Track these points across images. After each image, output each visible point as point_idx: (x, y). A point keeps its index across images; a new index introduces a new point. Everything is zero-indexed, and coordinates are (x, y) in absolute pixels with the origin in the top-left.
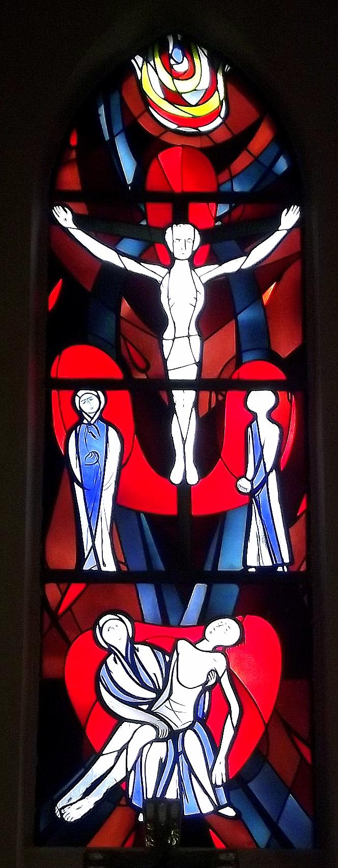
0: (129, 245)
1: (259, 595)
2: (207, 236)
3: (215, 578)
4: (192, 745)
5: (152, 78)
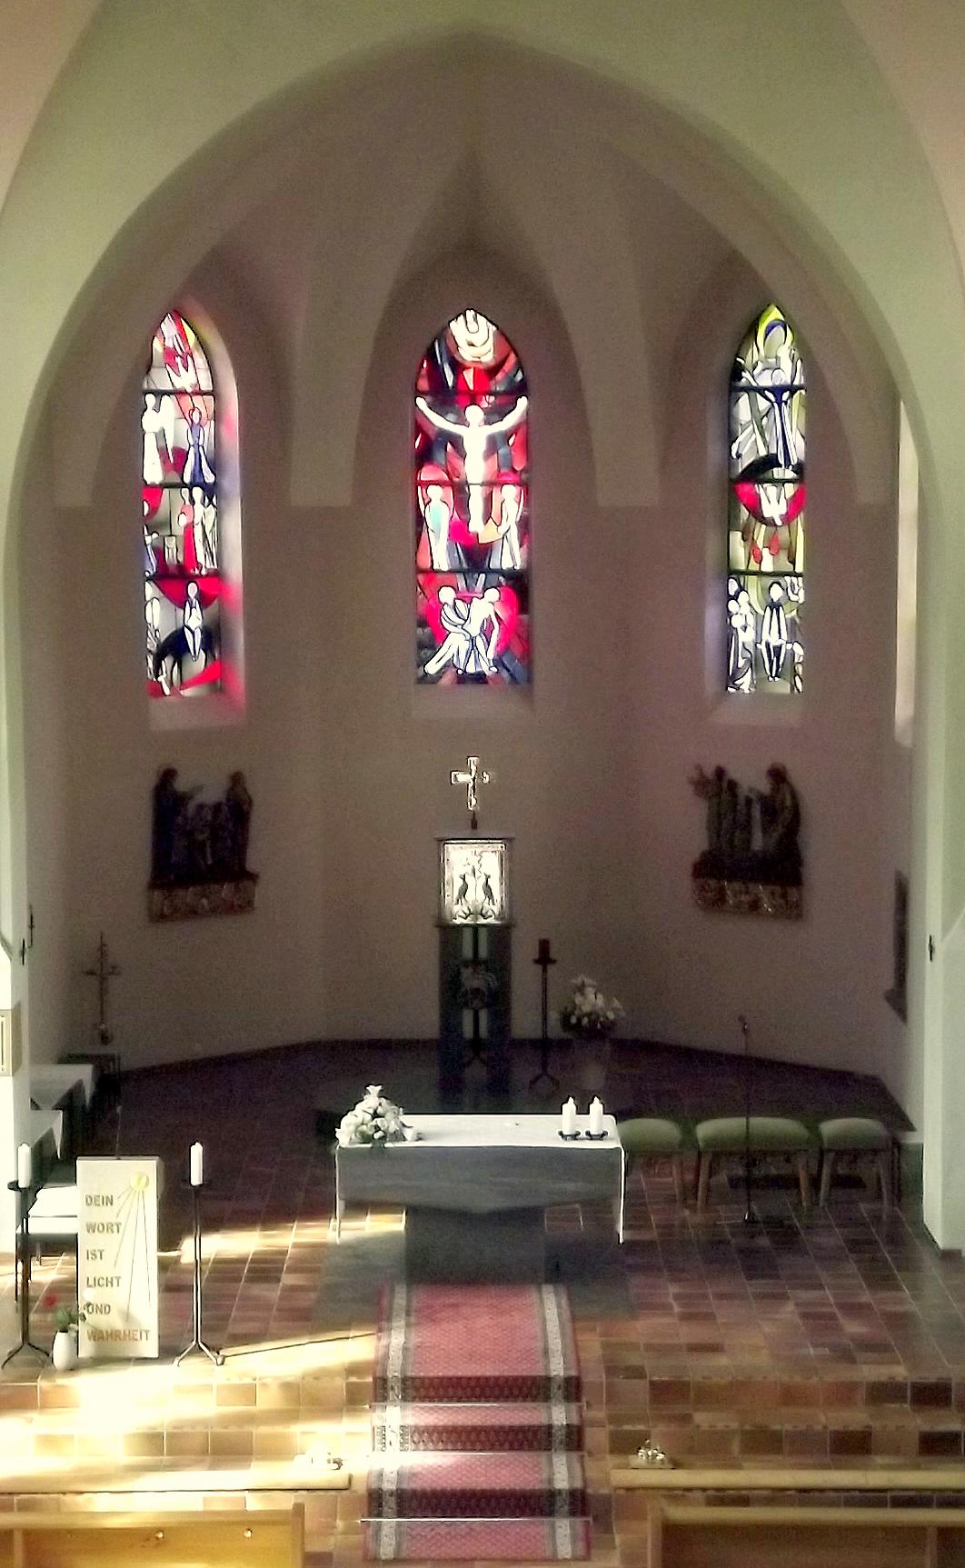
0: (451, 417)
2: (486, 411)
3: (489, 571)
4: (480, 643)
5: (457, 328)
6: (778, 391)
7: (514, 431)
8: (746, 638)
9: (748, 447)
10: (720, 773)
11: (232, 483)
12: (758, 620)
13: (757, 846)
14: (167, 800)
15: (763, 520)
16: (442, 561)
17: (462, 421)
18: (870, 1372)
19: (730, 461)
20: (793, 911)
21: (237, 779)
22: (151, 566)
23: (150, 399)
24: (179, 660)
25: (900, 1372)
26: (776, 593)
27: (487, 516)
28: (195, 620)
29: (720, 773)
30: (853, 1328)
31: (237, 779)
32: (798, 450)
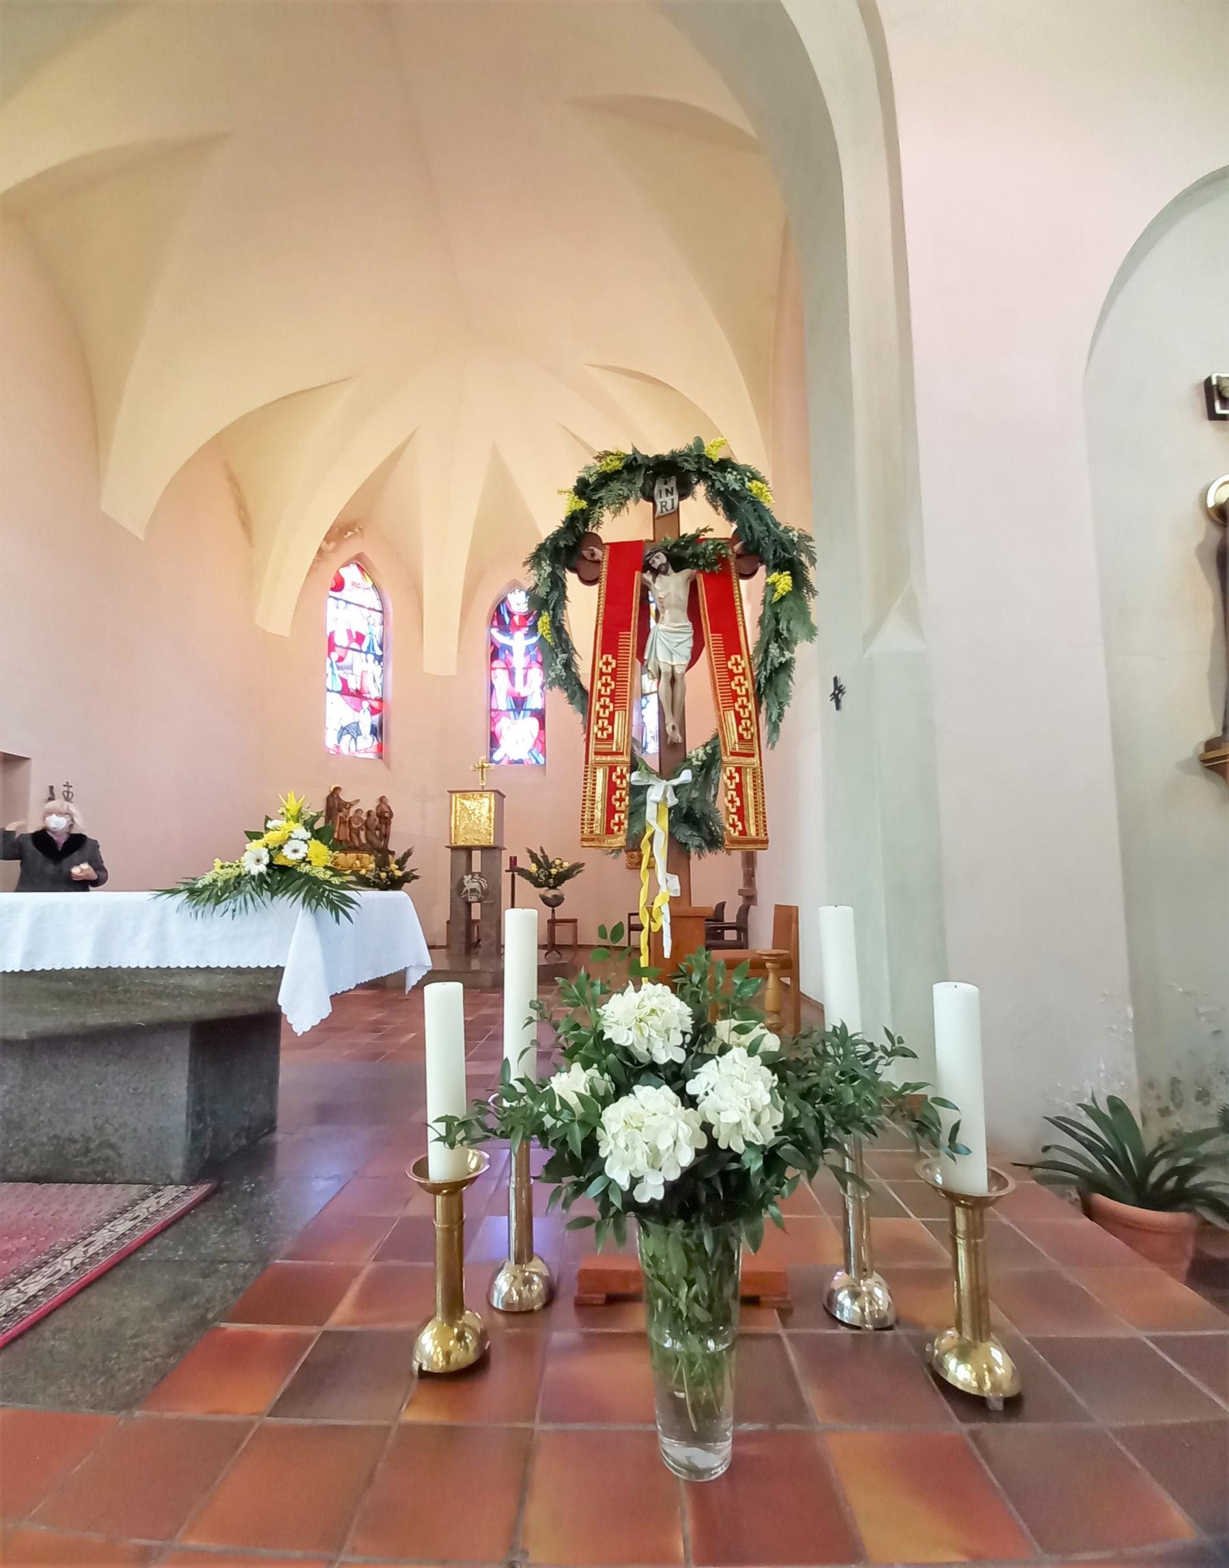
17: (512, 637)
21: (382, 800)
23: (342, 604)
28: (366, 720)
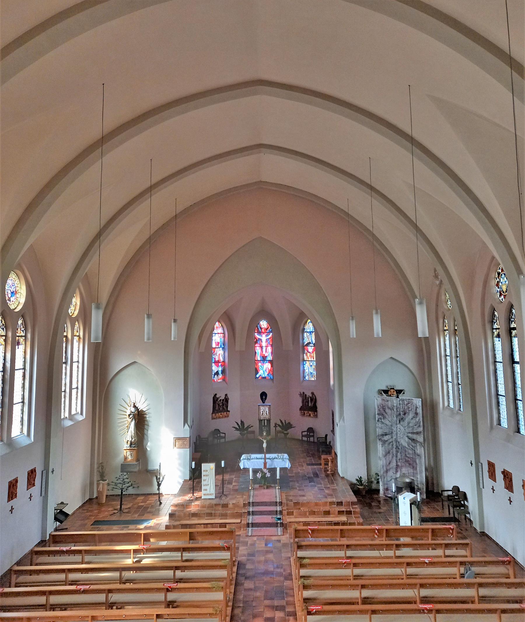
1: (270, 361)
5: (261, 323)
6: (310, 332)
7: (270, 338)
8: (307, 371)
9: (306, 341)
10: (304, 393)
11: (226, 347)
12: (309, 368)
13: (310, 405)
14: (215, 399)
15: (310, 352)
16: (259, 359)
17: (262, 336)
18: (330, 500)
19: (303, 343)
20: (316, 416)
21: (226, 395)
22: (213, 361)
24: (217, 376)
25: (334, 500)
26: (311, 364)
27: (266, 352)
28: (220, 369)
29: (304, 393)
30: (327, 491)
31: (226, 395)
32: (314, 342)
